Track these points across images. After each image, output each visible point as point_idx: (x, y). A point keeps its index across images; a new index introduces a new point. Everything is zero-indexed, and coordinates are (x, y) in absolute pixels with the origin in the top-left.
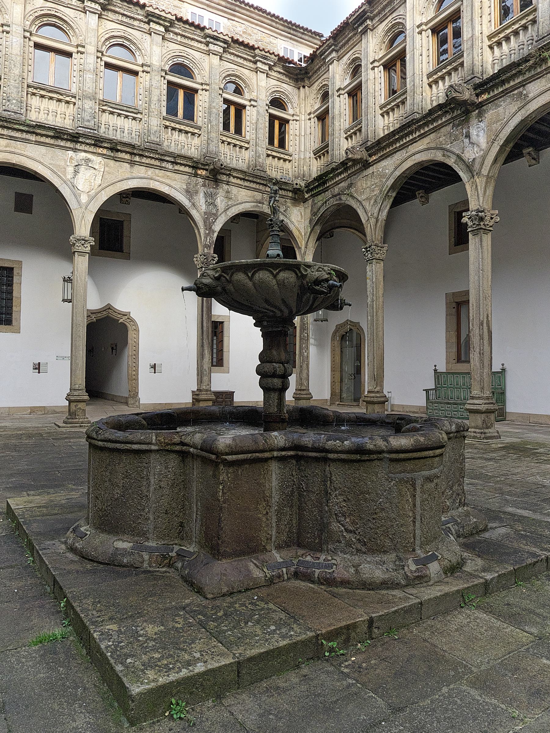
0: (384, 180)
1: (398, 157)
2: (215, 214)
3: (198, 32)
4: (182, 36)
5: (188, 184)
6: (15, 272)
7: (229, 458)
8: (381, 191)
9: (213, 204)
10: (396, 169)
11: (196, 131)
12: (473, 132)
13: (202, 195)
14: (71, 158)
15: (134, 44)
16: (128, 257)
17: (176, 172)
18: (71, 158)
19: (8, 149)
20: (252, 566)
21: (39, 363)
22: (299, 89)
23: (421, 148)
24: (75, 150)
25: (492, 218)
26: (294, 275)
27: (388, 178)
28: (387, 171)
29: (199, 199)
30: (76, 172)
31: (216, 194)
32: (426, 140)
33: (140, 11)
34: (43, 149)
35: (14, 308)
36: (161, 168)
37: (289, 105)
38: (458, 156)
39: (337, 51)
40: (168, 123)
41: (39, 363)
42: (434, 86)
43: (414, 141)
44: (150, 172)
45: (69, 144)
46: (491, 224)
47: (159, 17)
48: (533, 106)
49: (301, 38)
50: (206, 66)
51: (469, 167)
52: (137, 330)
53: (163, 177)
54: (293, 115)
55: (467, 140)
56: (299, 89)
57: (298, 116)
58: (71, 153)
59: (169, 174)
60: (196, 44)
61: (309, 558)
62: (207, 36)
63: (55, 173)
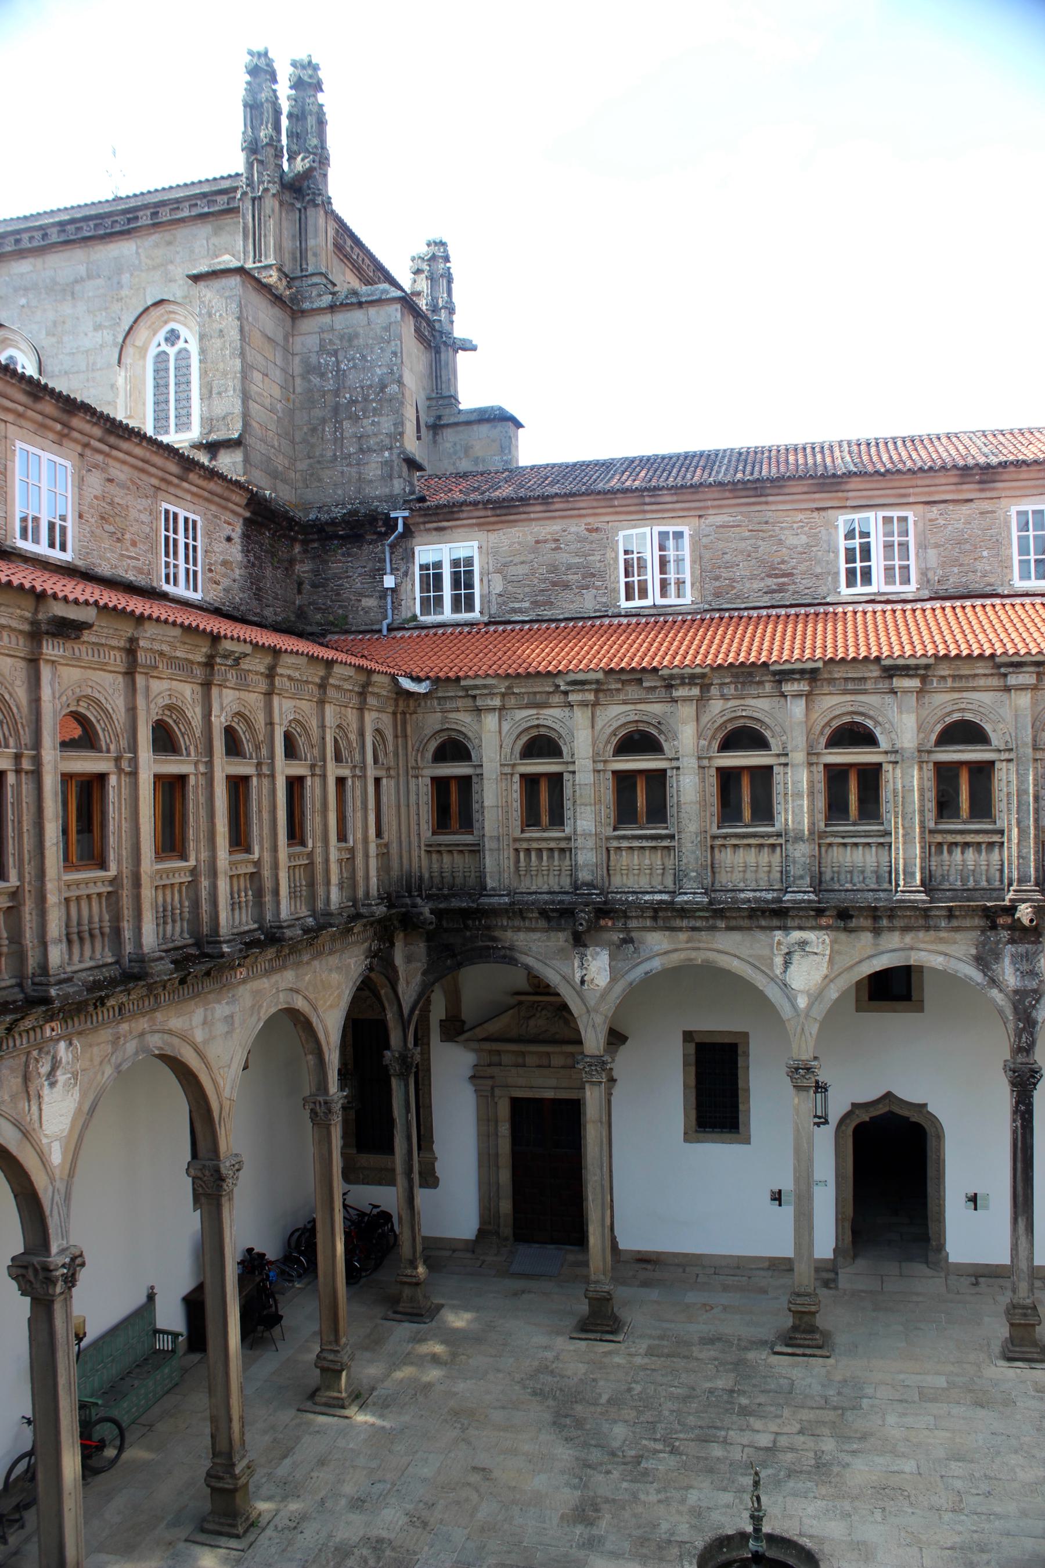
2: (1035, 991)
3: (980, 664)
4: (954, 677)
5: (981, 945)
6: (740, 1051)
9: (1033, 974)
11: (996, 838)
13: (1007, 961)
14: (779, 943)
15: (871, 718)
16: (920, 1008)
17: (957, 929)
18: (779, 943)
19: (689, 945)
21: (780, 1191)
24: (785, 928)
29: (1003, 969)
30: (787, 964)
31: (1036, 953)
33: (872, 667)
34: (736, 936)
35: (741, 1107)
36: (928, 928)
40: (939, 838)
41: (780, 1191)
44: (908, 938)
45: (775, 922)
47: (907, 667)
50: (1007, 713)
52: (940, 1136)
53: (932, 942)
58: (778, 935)
59: (943, 934)
60: (982, 682)
62: (999, 666)
63: (758, 969)
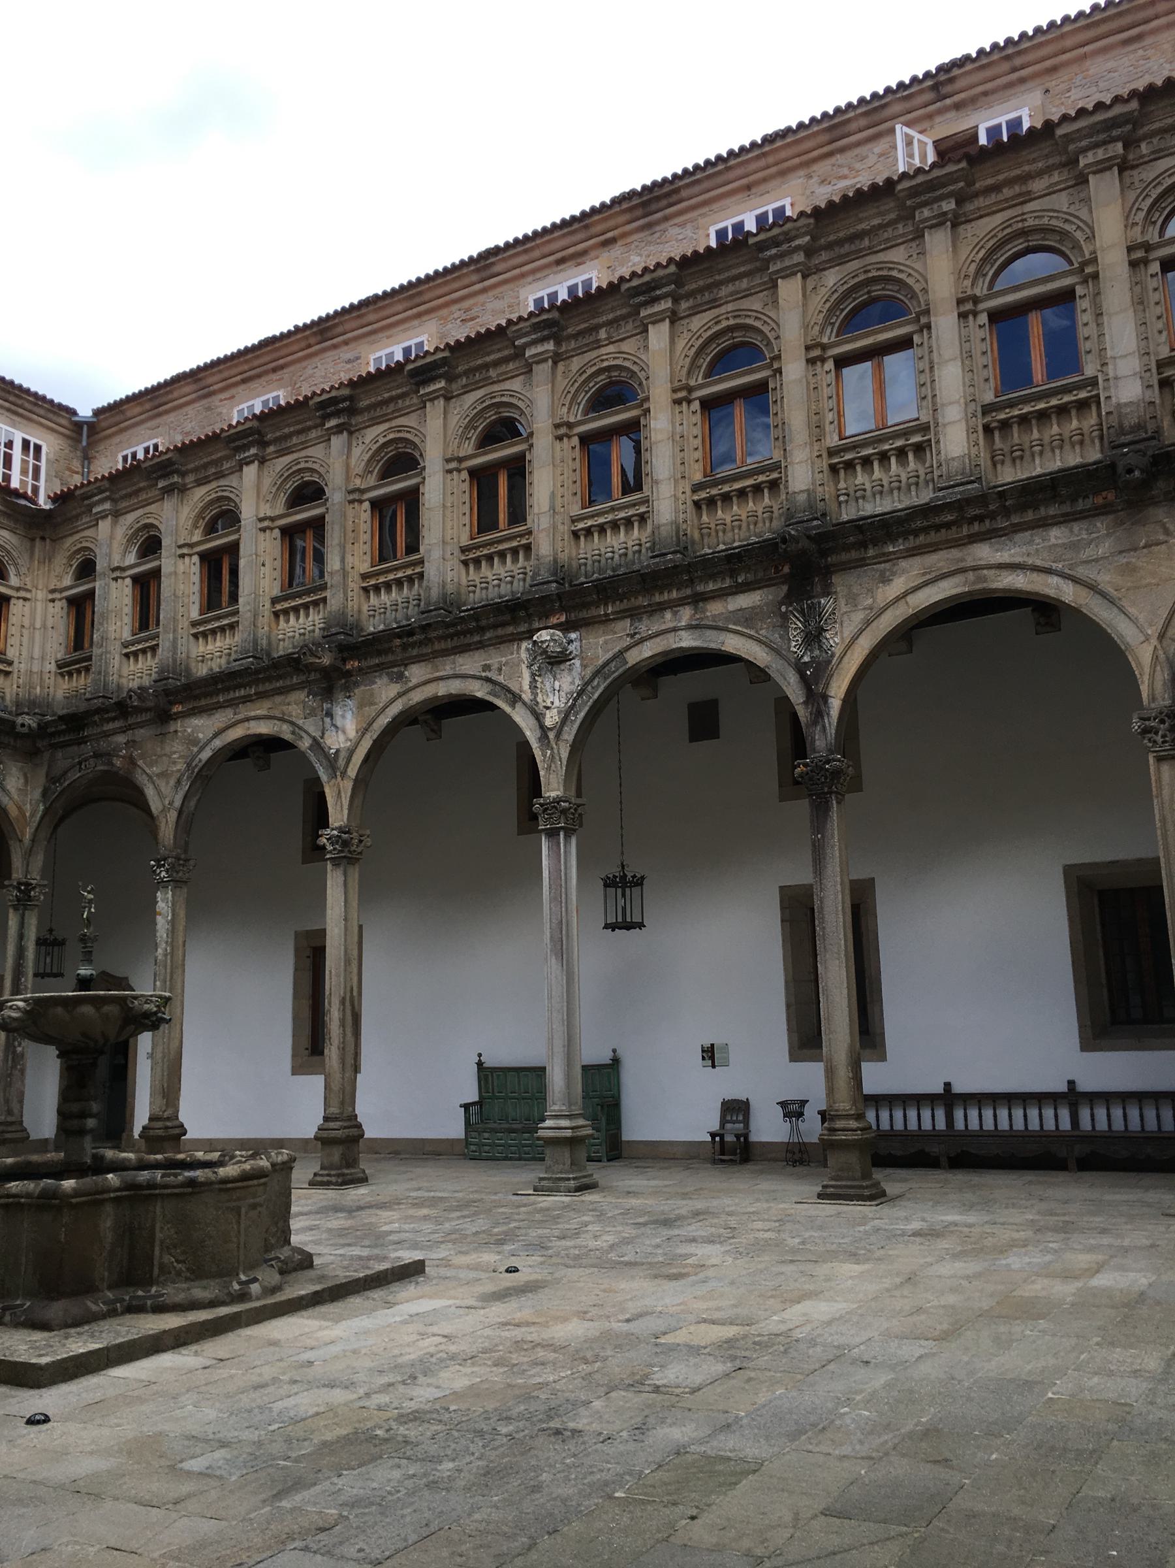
0: (195, 749)
1: (220, 718)
7: (74, 1200)
8: (189, 765)
10: (216, 735)
12: (338, 711)
20: (89, 1304)
22: (33, 540)
23: (259, 712)
25: (361, 841)
26: (118, 1007)
27: (202, 749)
28: (201, 736)
32: (267, 704)
37: (12, 571)
38: (314, 739)
39: (114, 501)
42: (282, 618)
43: (247, 699)
46: (359, 850)
48: (417, 697)
49: (30, 411)
51: (331, 762)
54: (18, 589)
55: (328, 720)
56: (33, 540)
57: (29, 591)
61: (140, 1293)
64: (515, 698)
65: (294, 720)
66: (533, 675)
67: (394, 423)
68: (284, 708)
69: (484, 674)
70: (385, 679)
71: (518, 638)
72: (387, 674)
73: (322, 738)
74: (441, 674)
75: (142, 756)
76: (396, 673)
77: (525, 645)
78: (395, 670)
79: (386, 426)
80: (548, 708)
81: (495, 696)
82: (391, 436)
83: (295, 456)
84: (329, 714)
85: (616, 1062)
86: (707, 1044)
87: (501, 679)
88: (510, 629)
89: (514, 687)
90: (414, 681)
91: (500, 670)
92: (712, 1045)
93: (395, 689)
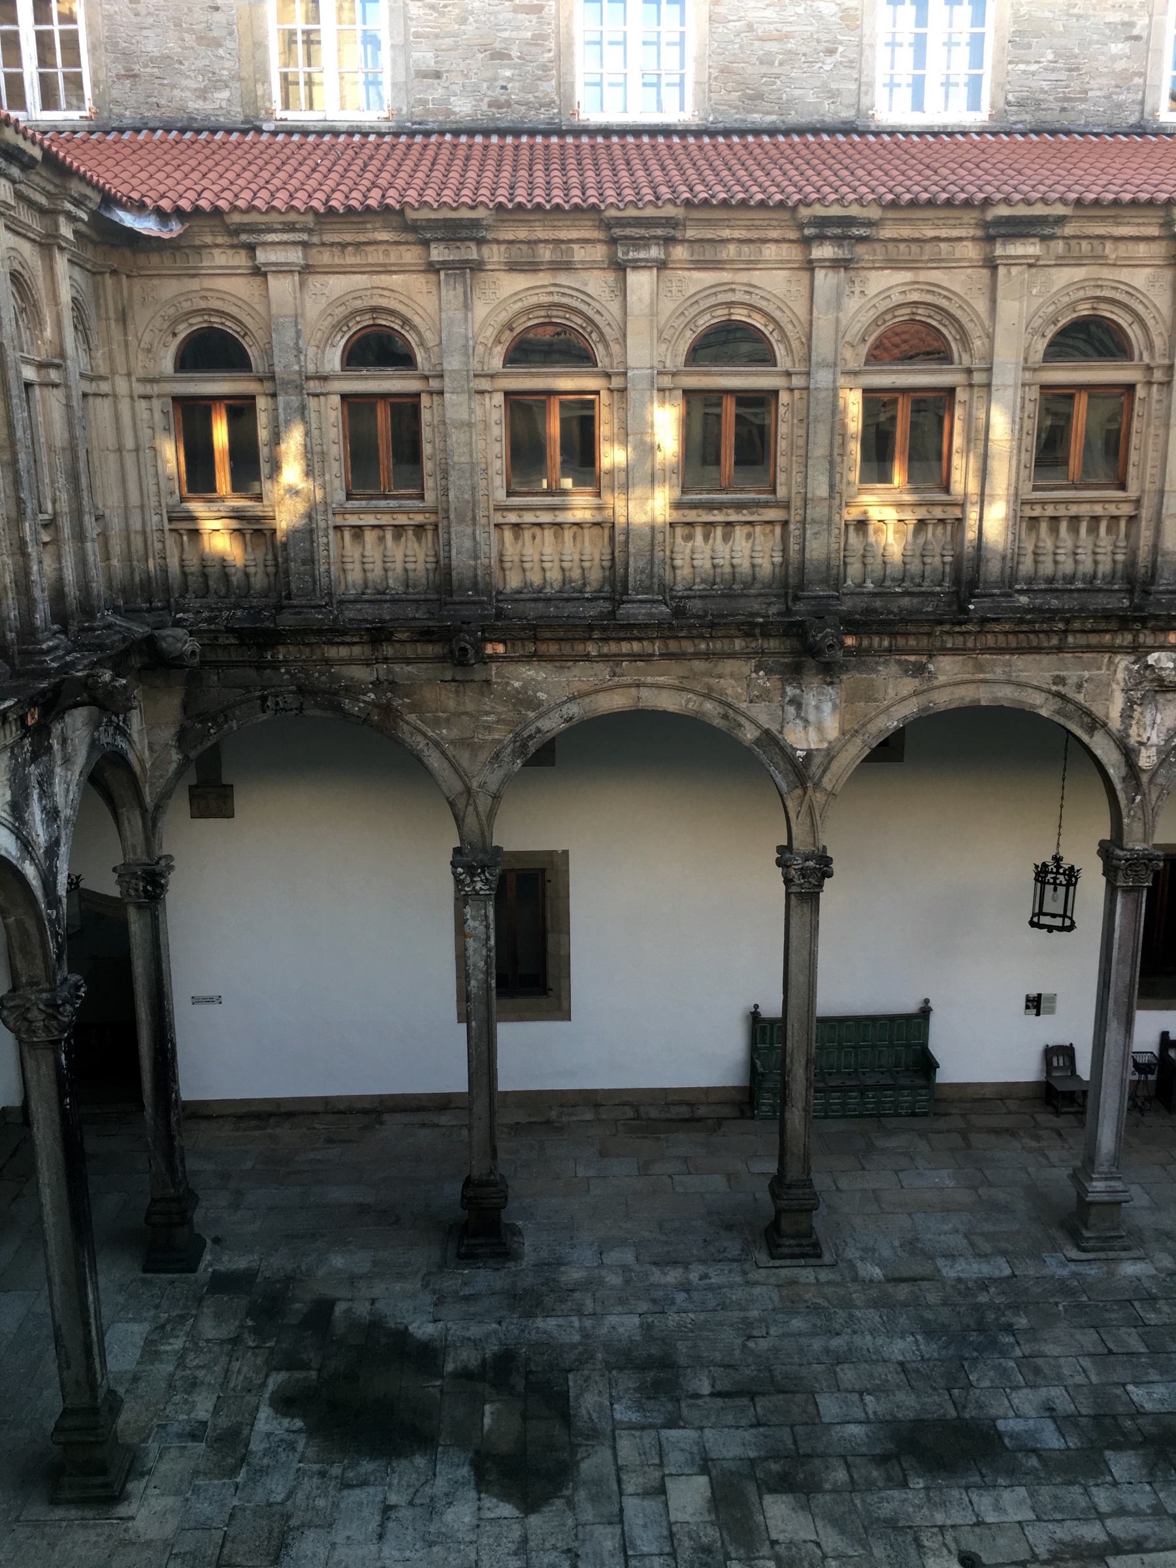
10: (572, 699)
12: (810, 699)
55: (791, 710)
64: (1095, 724)
65: (730, 700)
66: (1130, 704)
67: (923, 276)
68: (713, 681)
69: (1054, 688)
70: (894, 669)
71: (1113, 650)
72: (899, 662)
73: (781, 732)
74: (988, 676)
75: (413, 708)
76: (914, 664)
77: (1123, 662)
78: (912, 658)
79: (908, 276)
80: (1141, 744)
81: (1065, 716)
82: (915, 297)
83: (725, 276)
84: (797, 703)
85: (925, 1012)
86: (1033, 993)
87: (1080, 698)
88: (1107, 637)
89: (1097, 709)
90: (942, 679)
91: (1079, 686)
92: (1040, 995)
93: (909, 685)
